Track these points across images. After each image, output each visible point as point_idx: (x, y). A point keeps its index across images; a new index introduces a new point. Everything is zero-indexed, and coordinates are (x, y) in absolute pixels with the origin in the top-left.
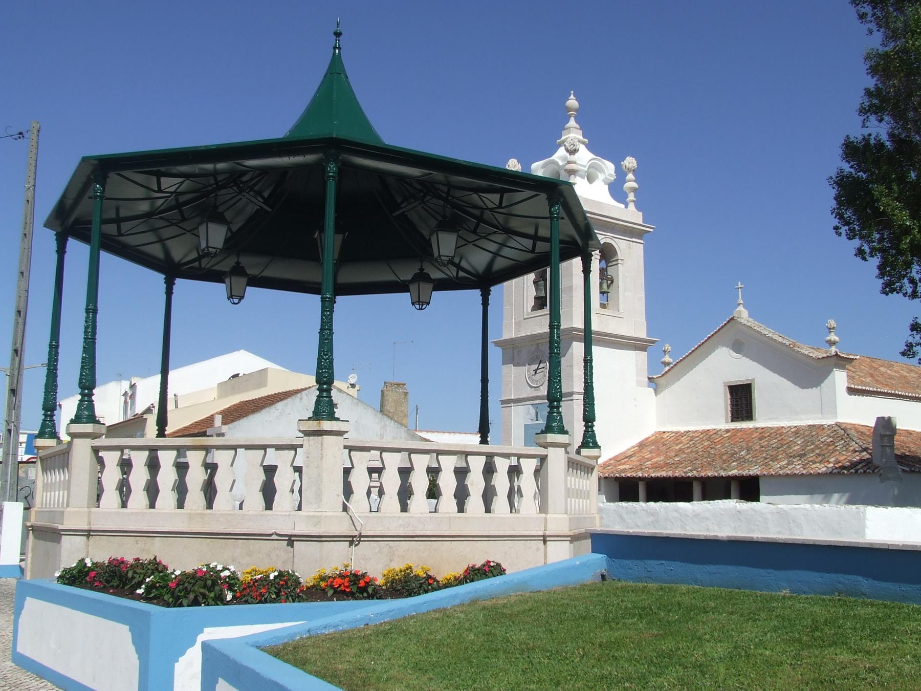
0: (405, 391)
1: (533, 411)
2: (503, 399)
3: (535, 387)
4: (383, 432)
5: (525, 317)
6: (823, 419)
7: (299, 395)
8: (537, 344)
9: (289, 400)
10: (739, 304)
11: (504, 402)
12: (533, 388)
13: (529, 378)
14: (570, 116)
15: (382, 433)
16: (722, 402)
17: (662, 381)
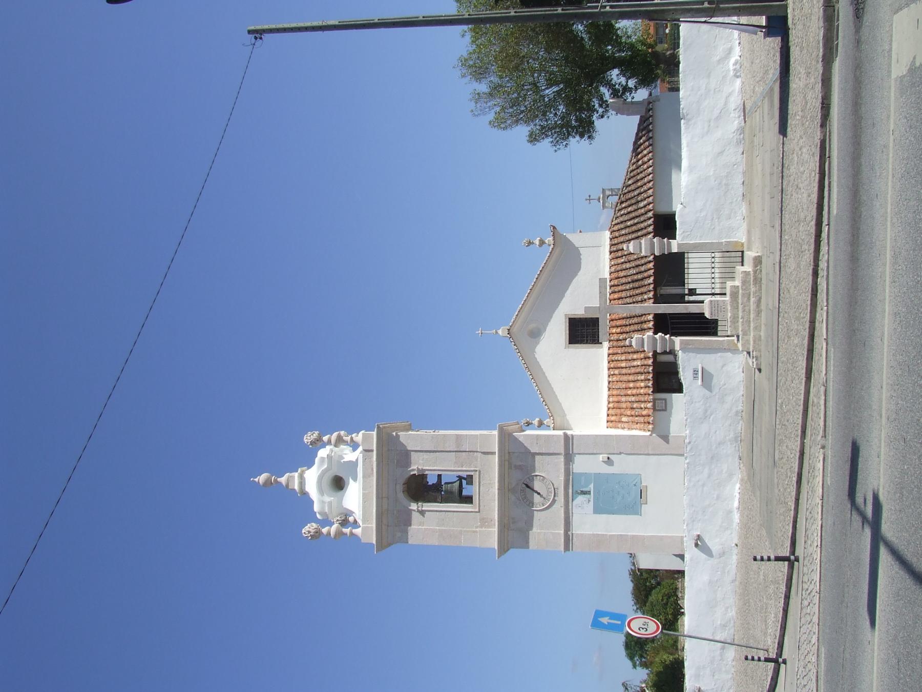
1: (580, 499)
2: (562, 548)
3: (555, 496)
5: (477, 510)
6: (605, 245)
8: (509, 490)
10: (496, 332)
11: (567, 547)
12: (556, 498)
13: (543, 506)
14: (276, 480)
16: (584, 351)
17: (558, 420)
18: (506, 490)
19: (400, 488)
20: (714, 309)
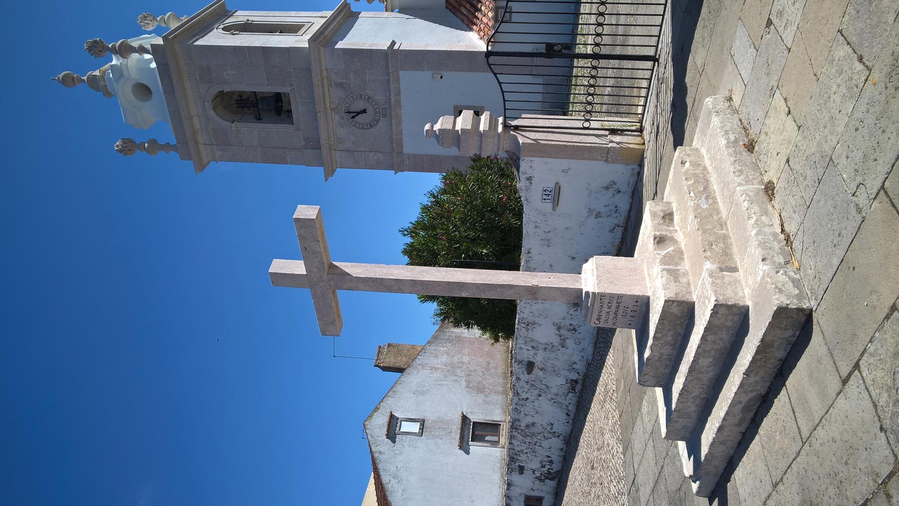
0: (386, 346)
4: (428, 367)
7: (376, 455)
8: (332, 110)
9: (380, 466)
15: (429, 368)
18: (329, 110)
19: (209, 106)
20: (605, 309)
